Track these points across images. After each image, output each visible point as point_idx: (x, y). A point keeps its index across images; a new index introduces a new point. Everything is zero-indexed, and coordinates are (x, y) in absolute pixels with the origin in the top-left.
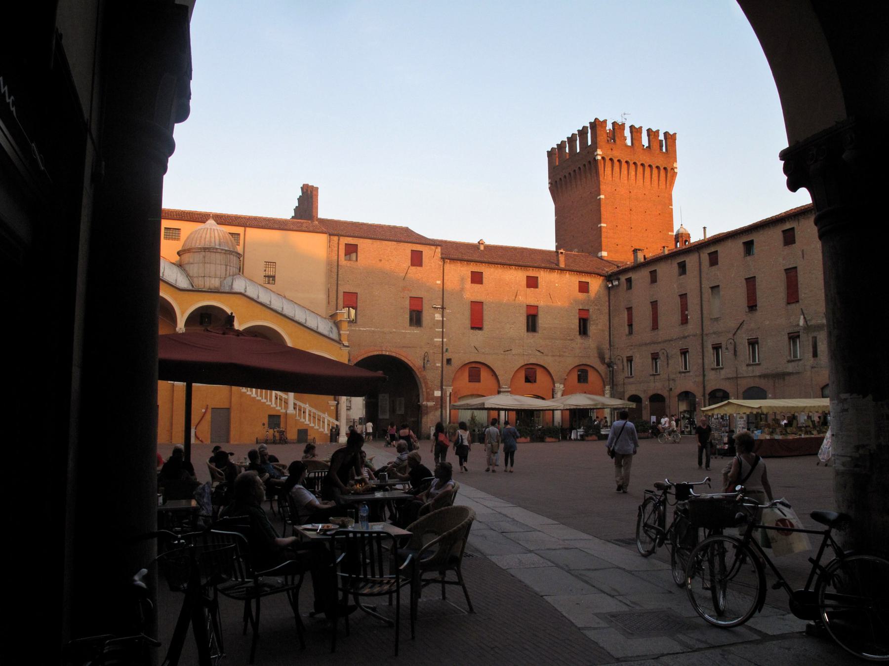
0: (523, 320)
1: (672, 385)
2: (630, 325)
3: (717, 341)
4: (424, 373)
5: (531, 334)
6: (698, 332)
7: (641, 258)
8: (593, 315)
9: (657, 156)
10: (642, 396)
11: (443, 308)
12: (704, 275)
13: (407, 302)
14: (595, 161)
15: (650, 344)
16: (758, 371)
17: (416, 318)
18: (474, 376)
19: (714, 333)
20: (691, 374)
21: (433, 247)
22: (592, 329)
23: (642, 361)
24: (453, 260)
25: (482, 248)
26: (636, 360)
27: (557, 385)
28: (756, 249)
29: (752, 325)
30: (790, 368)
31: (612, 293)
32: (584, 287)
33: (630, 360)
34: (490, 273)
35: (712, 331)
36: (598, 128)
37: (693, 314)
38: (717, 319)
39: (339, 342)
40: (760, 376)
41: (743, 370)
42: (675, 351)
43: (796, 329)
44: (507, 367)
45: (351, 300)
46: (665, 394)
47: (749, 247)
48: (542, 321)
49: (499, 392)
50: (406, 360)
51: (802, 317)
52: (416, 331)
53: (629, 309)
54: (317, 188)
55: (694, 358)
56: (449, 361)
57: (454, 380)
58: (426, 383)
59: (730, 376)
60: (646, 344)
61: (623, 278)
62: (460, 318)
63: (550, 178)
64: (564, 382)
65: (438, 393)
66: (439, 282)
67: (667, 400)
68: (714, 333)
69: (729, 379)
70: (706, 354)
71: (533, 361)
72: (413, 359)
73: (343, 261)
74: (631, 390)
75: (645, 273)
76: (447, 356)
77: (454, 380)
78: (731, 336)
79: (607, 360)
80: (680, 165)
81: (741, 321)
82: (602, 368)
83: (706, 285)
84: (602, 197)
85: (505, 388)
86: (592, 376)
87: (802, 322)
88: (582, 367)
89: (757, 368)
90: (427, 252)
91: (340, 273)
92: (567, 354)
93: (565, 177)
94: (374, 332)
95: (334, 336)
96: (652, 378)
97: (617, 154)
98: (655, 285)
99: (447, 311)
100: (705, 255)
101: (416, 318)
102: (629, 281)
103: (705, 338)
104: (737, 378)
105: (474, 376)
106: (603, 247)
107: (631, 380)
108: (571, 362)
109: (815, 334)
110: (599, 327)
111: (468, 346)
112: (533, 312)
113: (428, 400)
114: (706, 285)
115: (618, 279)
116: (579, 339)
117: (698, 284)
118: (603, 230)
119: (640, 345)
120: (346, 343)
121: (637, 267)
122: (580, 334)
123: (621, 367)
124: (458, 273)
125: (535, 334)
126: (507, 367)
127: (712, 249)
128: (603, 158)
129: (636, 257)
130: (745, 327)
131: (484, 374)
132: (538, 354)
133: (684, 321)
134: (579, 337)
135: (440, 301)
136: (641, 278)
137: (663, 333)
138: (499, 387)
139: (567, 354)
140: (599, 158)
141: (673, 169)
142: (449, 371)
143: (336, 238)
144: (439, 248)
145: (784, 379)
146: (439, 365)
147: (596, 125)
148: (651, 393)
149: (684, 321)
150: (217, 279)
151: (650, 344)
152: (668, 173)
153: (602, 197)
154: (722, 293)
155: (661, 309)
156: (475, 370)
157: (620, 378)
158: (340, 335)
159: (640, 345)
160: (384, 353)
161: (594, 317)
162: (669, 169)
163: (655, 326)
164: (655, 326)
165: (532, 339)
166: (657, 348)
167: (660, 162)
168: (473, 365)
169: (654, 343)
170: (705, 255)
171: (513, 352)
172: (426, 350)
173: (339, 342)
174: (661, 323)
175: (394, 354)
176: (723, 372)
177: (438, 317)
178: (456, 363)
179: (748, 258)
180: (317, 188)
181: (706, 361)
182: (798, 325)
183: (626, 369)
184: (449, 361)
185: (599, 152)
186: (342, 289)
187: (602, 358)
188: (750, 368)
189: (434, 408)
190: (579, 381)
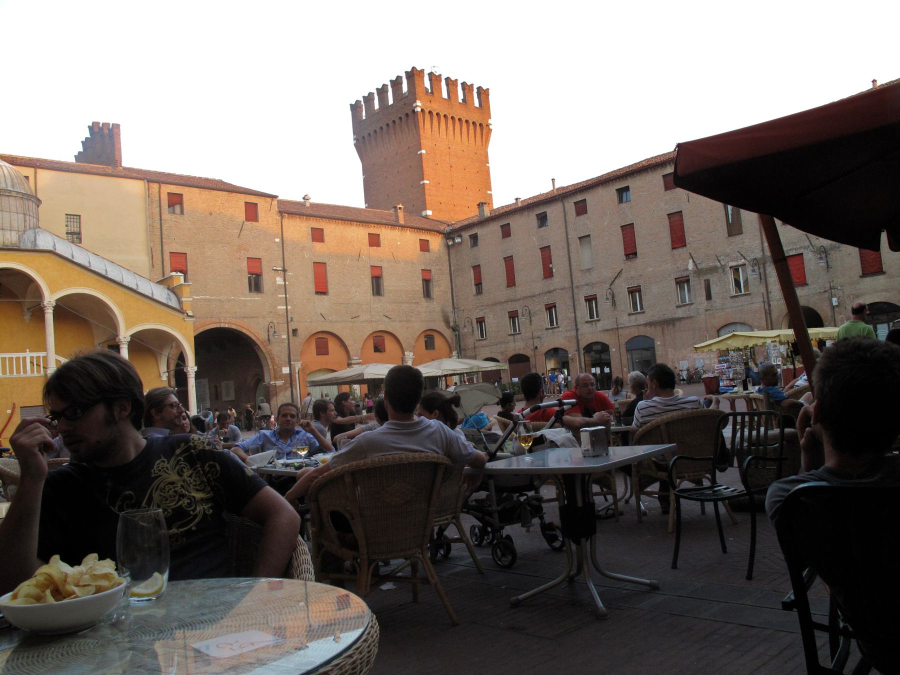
0: (368, 282)
1: (537, 343)
3: (590, 293)
4: (269, 347)
5: (377, 298)
6: (567, 284)
8: (435, 276)
9: (471, 112)
10: (499, 357)
11: (284, 270)
12: (570, 226)
13: (245, 264)
16: (642, 319)
17: (255, 285)
18: (322, 349)
19: (587, 285)
20: (560, 329)
21: (269, 200)
22: (436, 291)
23: (497, 322)
24: (292, 214)
25: (308, 205)
27: (407, 353)
28: (632, 194)
29: (633, 273)
30: (680, 313)
32: (424, 246)
33: (481, 321)
34: (331, 230)
35: (583, 283)
36: (416, 78)
37: (559, 264)
38: (589, 270)
39: (181, 311)
40: (646, 325)
41: (625, 320)
42: (539, 307)
43: (685, 274)
44: (356, 336)
45: (180, 263)
46: (529, 353)
47: (622, 192)
48: (388, 283)
49: (349, 365)
50: (248, 333)
51: (691, 261)
52: (256, 297)
53: (477, 269)
54: (117, 126)
55: (564, 312)
56: (295, 331)
57: (302, 353)
58: (272, 359)
59: (609, 327)
60: (501, 303)
61: (466, 235)
62: (304, 281)
63: (354, 133)
64: (414, 349)
65: (286, 370)
66: (277, 240)
67: (532, 360)
68: (587, 285)
69: (607, 330)
70: (578, 307)
71: (381, 327)
72: (255, 330)
73: (166, 215)
75: (495, 228)
76: (292, 326)
77: (302, 353)
78: (608, 286)
79: (452, 324)
80: (495, 122)
81: (618, 270)
82: (448, 333)
83: (574, 236)
84: (423, 151)
85: (355, 359)
86: (438, 342)
87: (691, 266)
88: (429, 333)
89: (640, 317)
90: (262, 203)
91: (164, 229)
92: (413, 319)
93: (375, 131)
94: (209, 300)
95: (174, 303)
96: (511, 338)
97: (435, 107)
98: (475, 248)
99: (289, 274)
100: (570, 205)
101: (255, 285)
102: (474, 238)
103: (576, 291)
104: (617, 329)
105: (322, 349)
106: (428, 206)
107: (484, 342)
108: (419, 327)
109: (708, 277)
110: (442, 288)
111: (314, 314)
112: (377, 274)
113: (276, 379)
114: (574, 236)
115: (461, 236)
116: (424, 302)
117: (564, 235)
118: (426, 187)
120: (190, 313)
121: (483, 222)
123: (470, 330)
124: (298, 230)
125: (381, 298)
126: (356, 336)
127: (579, 198)
128: (422, 110)
129: (481, 211)
130: (623, 275)
131: (332, 345)
132: (386, 319)
133: (548, 273)
134: (423, 300)
135: (280, 262)
136: (490, 234)
137: (520, 290)
138: (349, 358)
139: (413, 319)
140: (419, 109)
141: (488, 126)
142: (296, 342)
143: (155, 186)
144: (275, 203)
145: (674, 325)
146: (285, 337)
147: (413, 75)
148: (511, 354)
149: (548, 273)
150: (14, 233)
152: (483, 130)
153: (423, 151)
154: (593, 243)
155: (517, 265)
156: (322, 341)
157: (469, 342)
158: (180, 302)
160: (222, 325)
162: (484, 126)
163: (511, 282)
164: (511, 282)
165: (378, 304)
167: (475, 117)
168: (320, 336)
169: (512, 301)
170: (570, 205)
171: (361, 318)
172: (269, 320)
173: (181, 311)
174: (519, 278)
175: (234, 327)
176: (600, 324)
177: (280, 281)
178: (303, 334)
179: (623, 205)
180: (117, 126)
181: (578, 314)
182: (687, 269)
184: (295, 331)
185: (419, 103)
186: (167, 250)
187: (447, 322)
188: (633, 317)
189: (284, 388)
190: (427, 347)
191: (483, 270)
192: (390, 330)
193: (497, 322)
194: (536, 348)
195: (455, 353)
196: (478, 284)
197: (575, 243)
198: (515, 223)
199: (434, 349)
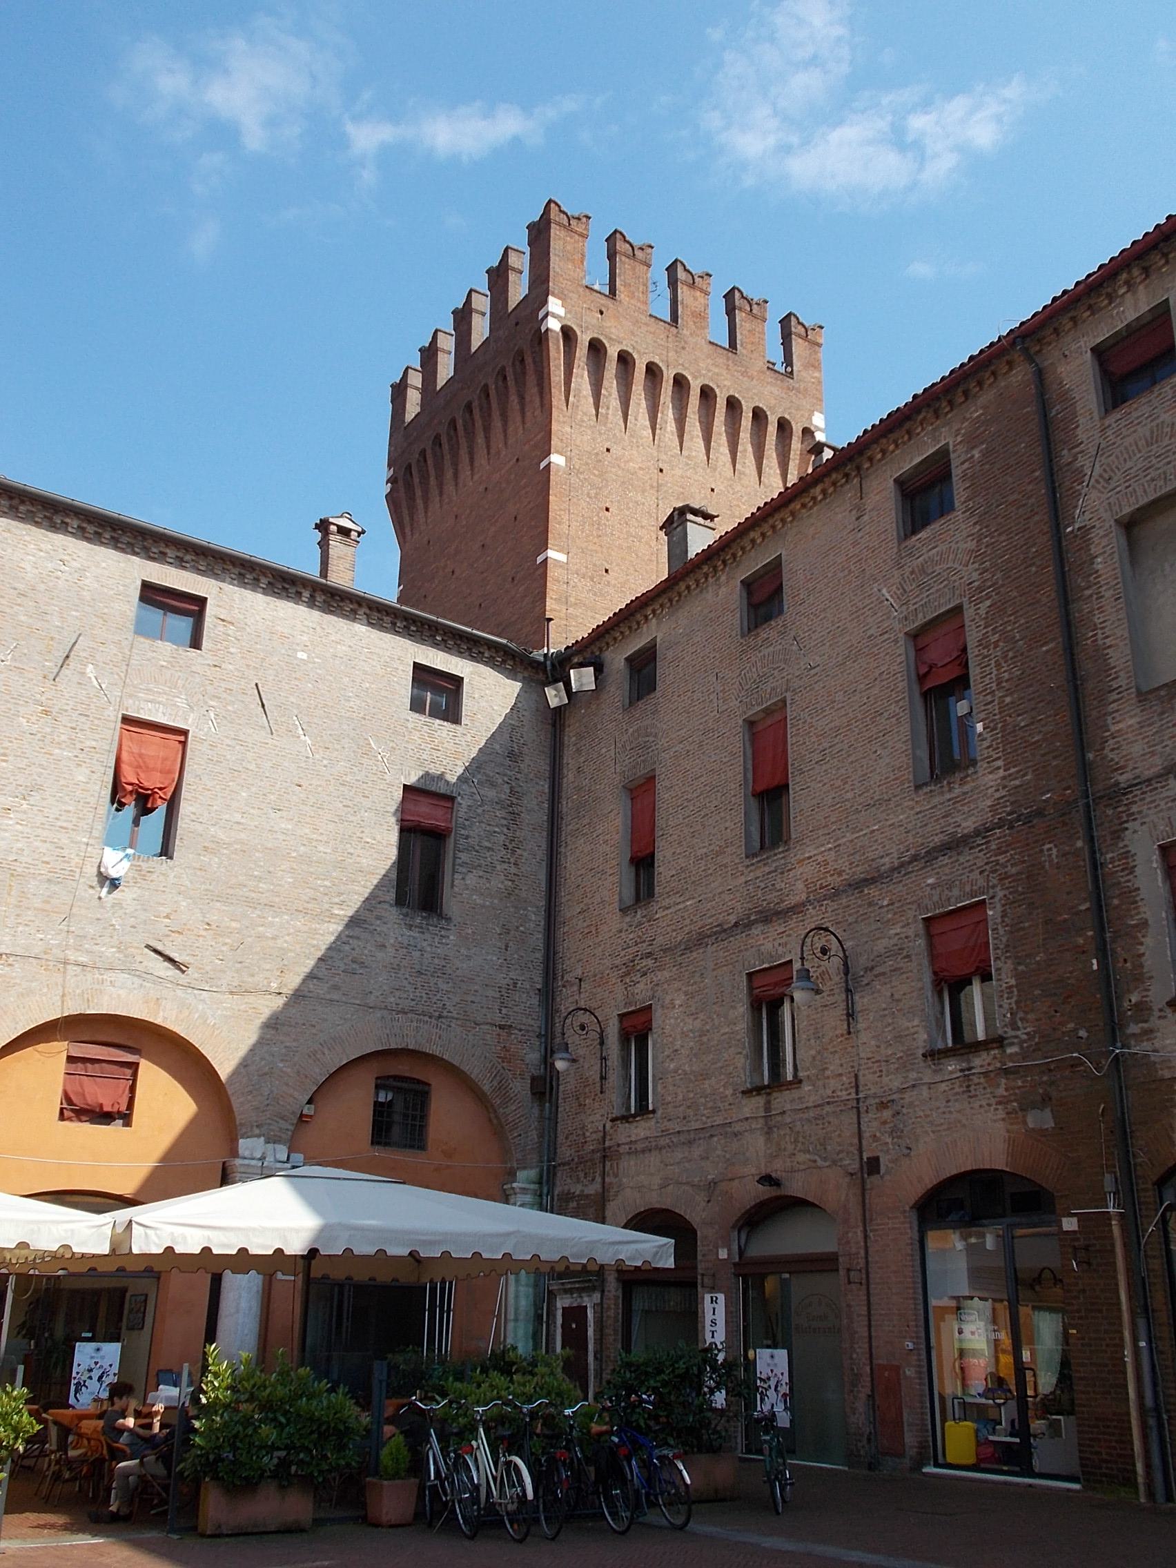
2: (643, 863)
7: (699, 539)
8: (474, 829)
10: (697, 1213)
14: (541, 338)
15: (743, 925)
22: (464, 888)
23: (698, 1031)
26: (672, 1028)
31: (570, 737)
32: (438, 695)
33: (637, 1029)
53: (642, 791)
60: (723, 932)
63: (389, 466)
74: (642, 1182)
86: (448, 1116)
88: (403, 1068)
100: (1075, 369)
107: (641, 1130)
118: (552, 573)
119: (699, 940)
122: (400, 901)
123: (594, 1073)
128: (567, 333)
151: (743, 925)
159: (699, 940)
161: (477, 832)
162: (797, 429)
166: (774, 944)
169: (768, 916)
183: (614, 1078)
191: (666, 795)
192: (167, 1017)
193: (698, 1031)
194: (873, 1166)
195: (525, 1178)
196: (643, 863)
197: (1106, 555)
198: (801, 552)
199: (422, 1147)
